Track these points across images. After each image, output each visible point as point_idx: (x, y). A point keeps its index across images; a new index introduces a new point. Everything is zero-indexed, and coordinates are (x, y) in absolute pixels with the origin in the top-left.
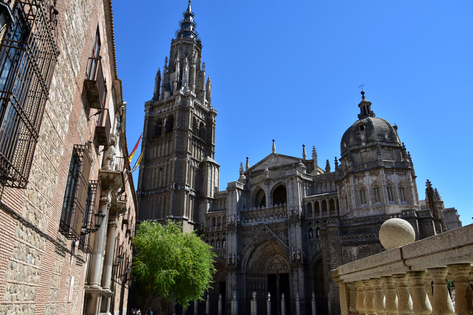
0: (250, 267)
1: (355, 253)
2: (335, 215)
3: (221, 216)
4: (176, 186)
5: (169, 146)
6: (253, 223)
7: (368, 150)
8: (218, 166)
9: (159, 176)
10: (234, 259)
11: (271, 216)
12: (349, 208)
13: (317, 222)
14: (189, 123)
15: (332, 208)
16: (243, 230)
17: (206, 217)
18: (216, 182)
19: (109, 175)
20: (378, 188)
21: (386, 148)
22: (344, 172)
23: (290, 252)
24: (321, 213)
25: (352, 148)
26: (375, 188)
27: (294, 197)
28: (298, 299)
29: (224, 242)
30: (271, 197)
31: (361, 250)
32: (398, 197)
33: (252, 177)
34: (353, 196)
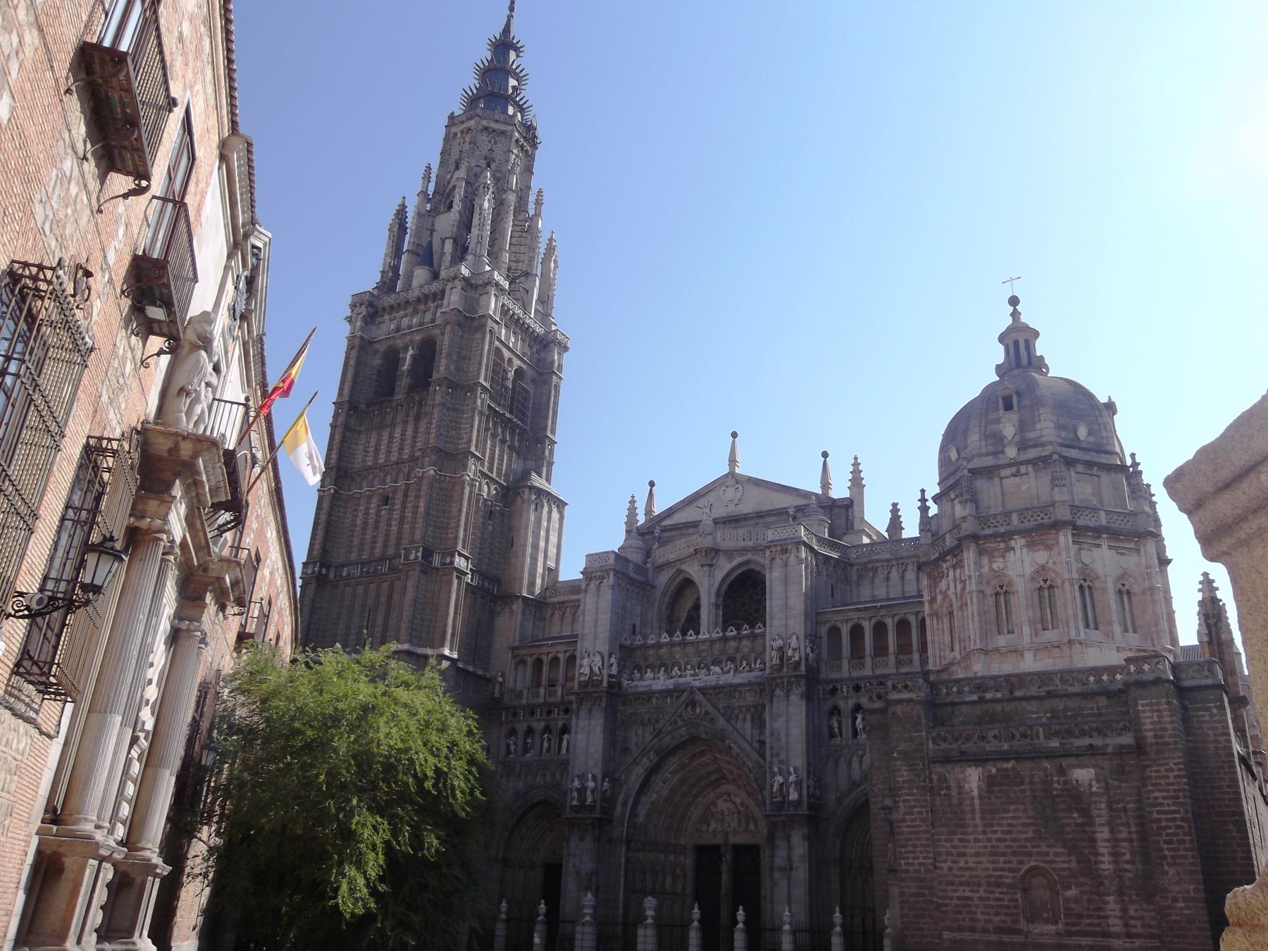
0: (641, 819)
2: (913, 670)
3: (561, 656)
4: (428, 554)
5: (416, 432)
6: (660, 682)
7: (1023, 469)
8: (561, 505)
9: (377, 521)
10: (593, 791)
11: (716, 662)
12: (957, 647)
13: (857, 688)
14: (480, 364)
15: (904, 648)
16: (624, 704)
17: (515, 657)
18: (552, 551)
19: (177, 444)
20: (1051, 587)
21: (1080, 468)
22: (948, 536)
23: (768, 775)
24: (868, 661)
25: (976, 463)
26: (1040, 589)
28: (787, 927)
29: (566, 736)
30: (717, 606)
31: (994, 777)
32: (1115, 616)
33: (663, 543)
34: (973, 608)
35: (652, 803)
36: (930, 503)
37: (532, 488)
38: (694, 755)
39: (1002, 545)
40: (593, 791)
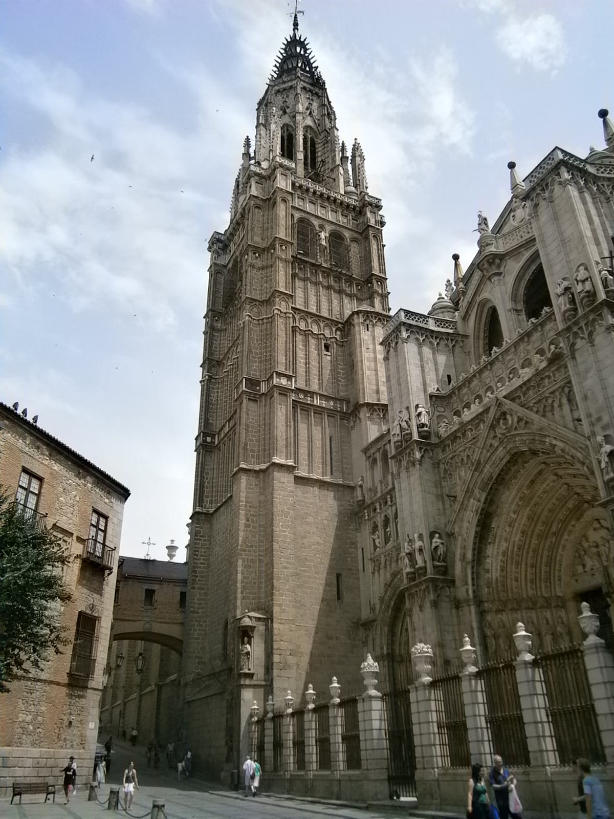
27: (563, 242)
35: (504, 554)
37: (358, 313)
38: (532, 482)
40: (421, 550)
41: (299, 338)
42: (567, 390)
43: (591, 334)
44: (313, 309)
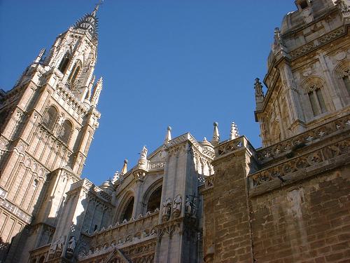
1: (297, 208)
7: (319, 25)
11: (138, 235)
36: (263, 84)
37: (62, 169)
39: (309, 61)
41: (23, 170)
42: (152, 257)
43: (171, 233)
44: (38, 157)
